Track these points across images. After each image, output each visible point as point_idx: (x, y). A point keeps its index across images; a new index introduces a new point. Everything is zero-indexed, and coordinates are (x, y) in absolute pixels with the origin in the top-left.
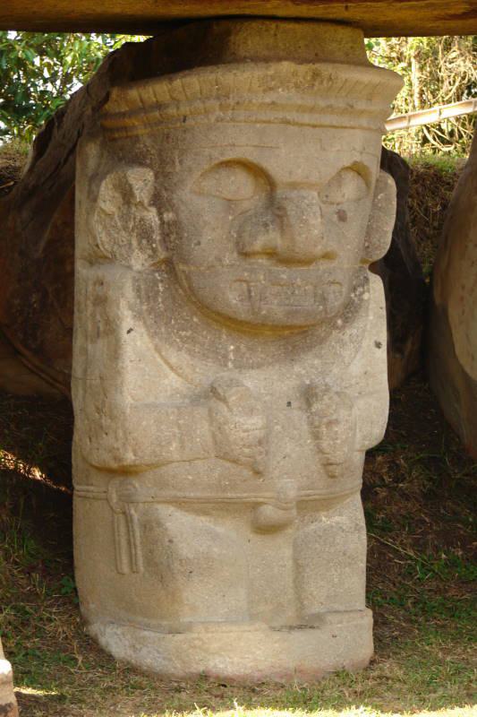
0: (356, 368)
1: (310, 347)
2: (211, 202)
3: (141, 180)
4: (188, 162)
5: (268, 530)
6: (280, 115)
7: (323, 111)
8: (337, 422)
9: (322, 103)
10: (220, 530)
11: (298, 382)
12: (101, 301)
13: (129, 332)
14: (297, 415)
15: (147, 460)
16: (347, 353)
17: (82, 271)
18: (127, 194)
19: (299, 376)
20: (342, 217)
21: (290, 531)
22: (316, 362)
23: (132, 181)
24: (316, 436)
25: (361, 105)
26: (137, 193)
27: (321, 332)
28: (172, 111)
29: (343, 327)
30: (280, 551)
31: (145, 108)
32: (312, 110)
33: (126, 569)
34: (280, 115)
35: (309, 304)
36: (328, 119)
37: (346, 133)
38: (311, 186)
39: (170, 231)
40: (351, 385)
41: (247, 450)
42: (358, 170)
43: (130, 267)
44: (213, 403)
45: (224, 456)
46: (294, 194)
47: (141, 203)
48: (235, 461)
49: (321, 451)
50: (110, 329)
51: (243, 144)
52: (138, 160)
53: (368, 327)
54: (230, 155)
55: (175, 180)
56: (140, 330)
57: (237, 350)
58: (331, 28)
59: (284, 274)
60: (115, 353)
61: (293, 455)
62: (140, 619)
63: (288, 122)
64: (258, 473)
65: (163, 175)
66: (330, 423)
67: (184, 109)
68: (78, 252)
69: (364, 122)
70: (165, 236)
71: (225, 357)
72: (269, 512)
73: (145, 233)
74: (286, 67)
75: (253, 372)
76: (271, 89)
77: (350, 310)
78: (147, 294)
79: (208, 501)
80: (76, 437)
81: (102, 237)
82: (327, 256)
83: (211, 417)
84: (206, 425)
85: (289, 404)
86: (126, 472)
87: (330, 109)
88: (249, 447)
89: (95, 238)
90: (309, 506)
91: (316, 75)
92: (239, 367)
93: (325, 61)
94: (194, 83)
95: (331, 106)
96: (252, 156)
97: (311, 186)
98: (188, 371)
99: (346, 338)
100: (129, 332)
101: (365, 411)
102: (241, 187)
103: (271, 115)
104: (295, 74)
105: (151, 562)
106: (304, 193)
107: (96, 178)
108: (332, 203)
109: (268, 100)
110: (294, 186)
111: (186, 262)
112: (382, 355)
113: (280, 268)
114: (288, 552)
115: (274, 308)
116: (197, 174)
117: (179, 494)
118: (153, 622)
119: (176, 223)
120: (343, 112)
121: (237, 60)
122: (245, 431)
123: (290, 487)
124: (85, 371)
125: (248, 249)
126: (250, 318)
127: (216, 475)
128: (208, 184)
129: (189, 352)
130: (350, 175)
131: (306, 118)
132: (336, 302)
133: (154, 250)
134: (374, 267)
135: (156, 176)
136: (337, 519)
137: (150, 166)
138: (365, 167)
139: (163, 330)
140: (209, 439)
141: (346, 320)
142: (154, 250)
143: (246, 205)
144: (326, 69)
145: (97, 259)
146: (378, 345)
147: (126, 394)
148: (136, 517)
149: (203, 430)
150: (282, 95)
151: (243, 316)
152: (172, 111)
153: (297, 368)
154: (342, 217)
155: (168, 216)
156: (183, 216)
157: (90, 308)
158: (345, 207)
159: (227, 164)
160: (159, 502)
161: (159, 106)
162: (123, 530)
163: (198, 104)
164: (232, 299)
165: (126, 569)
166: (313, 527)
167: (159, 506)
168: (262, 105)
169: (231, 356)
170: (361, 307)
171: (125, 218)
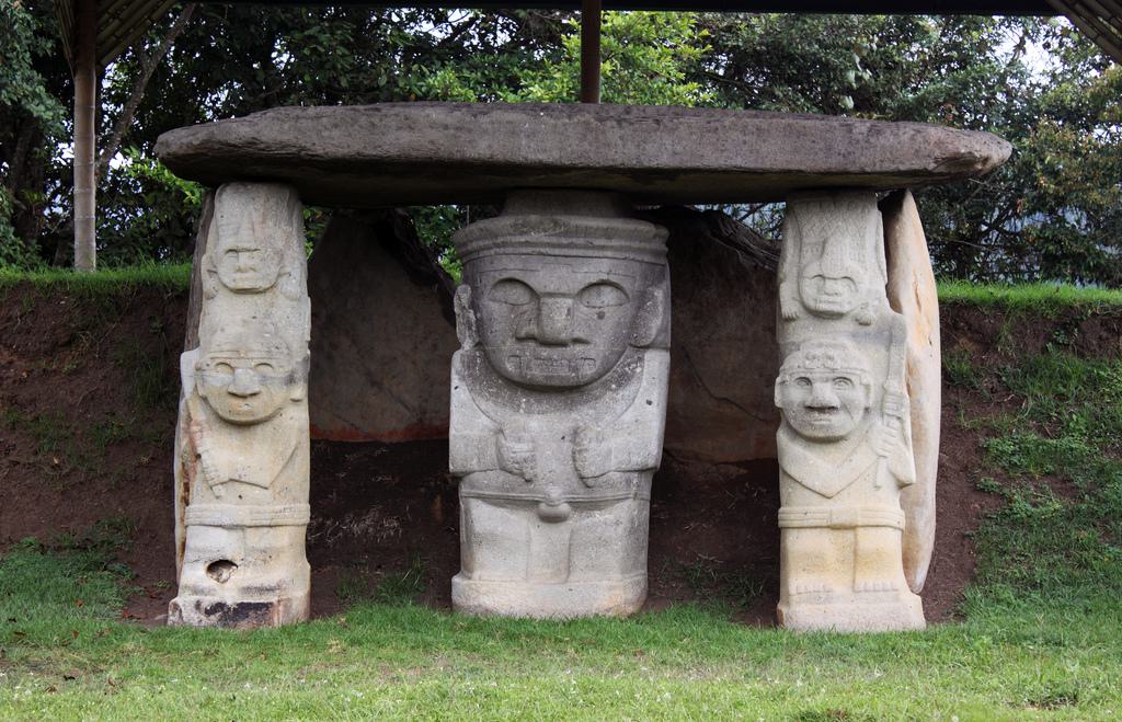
1: (587, 402)
2: (496, 307)
4: (483, 282)
5: (552, 519)
6: (538, 249)
8: (586, 450)
9: (564, 241)
10: (513, 517)
11: (573, 424)
13: (456, 388)
14: (567, 446)
16: (619, 408)
19: (575, 420)
20: (601, 316)
22: (591, 412)
24: (574, 460)
29: (616, 390)
30: (561, 533)
35: (564, 372)
37: (595, 260)
40: (622, 428)
41: (517, 466)
45: (504, 469)
46: (550, 301)
48: (511, 472)
49: (576, 470)
51: (511, 266)
53: (641, 390)
54: (505, 275)
55: (480, 291)
57: (528, 401)
59: (545, 352)
61: (558, 471)
64: (528, 481)
65: (474, 289)
66: (580, 451)
67: (474, 245)
69: (609, 254)
70: (477, 327)
71: (519, 406)
73: (470, 328)
74: (533, 218)
75: (539, 417)
76: (526, 233)
77: (614, 374)
78: (469, 364)
79: (498, 498)
82: (577, 341)
85: (563, 438)
87: (576, 246)
88: (518, 463)
90: (583, 506)
91: (556, 223)
92: (529, 412)
95: (572, 243)
96: (519, 276)
97: (564, 295)
98: (492, 414)
99: (619, 397)
100: (456, 388)
103: (530, 250)
106: (559, 300)
108: (594, 307)
109: (523, 240)
110: (551, 295)
113: (543, 349)
115: (537, 373)
116: (489, 288)
117: (481, 492)
120: (585, 247)
122: (514, 452)
125: (518, 336)
126: (520, 380)
127: (501, 479)
129: (495, 403)
131: (557, 251)
135: (472, 290)
136: (607, 516)
139: (478, 387)
140: (494, 456)
141: (620, 385)
143: (525, 308)
144: (563, 219)
146: (649, 403)
149: (492, 451)
150: (533, 237)
151: (516, 379)
153: (574, 415)
154: (601, 316)
158: (605, 310)
159: (512, 281)
160: (479, 497)
163: (481, 243)
164: (510, 367)
166: (588, 520)
167: (472, 500)
168: (519, 243)
169: (523, 406)
170: (633, 376)
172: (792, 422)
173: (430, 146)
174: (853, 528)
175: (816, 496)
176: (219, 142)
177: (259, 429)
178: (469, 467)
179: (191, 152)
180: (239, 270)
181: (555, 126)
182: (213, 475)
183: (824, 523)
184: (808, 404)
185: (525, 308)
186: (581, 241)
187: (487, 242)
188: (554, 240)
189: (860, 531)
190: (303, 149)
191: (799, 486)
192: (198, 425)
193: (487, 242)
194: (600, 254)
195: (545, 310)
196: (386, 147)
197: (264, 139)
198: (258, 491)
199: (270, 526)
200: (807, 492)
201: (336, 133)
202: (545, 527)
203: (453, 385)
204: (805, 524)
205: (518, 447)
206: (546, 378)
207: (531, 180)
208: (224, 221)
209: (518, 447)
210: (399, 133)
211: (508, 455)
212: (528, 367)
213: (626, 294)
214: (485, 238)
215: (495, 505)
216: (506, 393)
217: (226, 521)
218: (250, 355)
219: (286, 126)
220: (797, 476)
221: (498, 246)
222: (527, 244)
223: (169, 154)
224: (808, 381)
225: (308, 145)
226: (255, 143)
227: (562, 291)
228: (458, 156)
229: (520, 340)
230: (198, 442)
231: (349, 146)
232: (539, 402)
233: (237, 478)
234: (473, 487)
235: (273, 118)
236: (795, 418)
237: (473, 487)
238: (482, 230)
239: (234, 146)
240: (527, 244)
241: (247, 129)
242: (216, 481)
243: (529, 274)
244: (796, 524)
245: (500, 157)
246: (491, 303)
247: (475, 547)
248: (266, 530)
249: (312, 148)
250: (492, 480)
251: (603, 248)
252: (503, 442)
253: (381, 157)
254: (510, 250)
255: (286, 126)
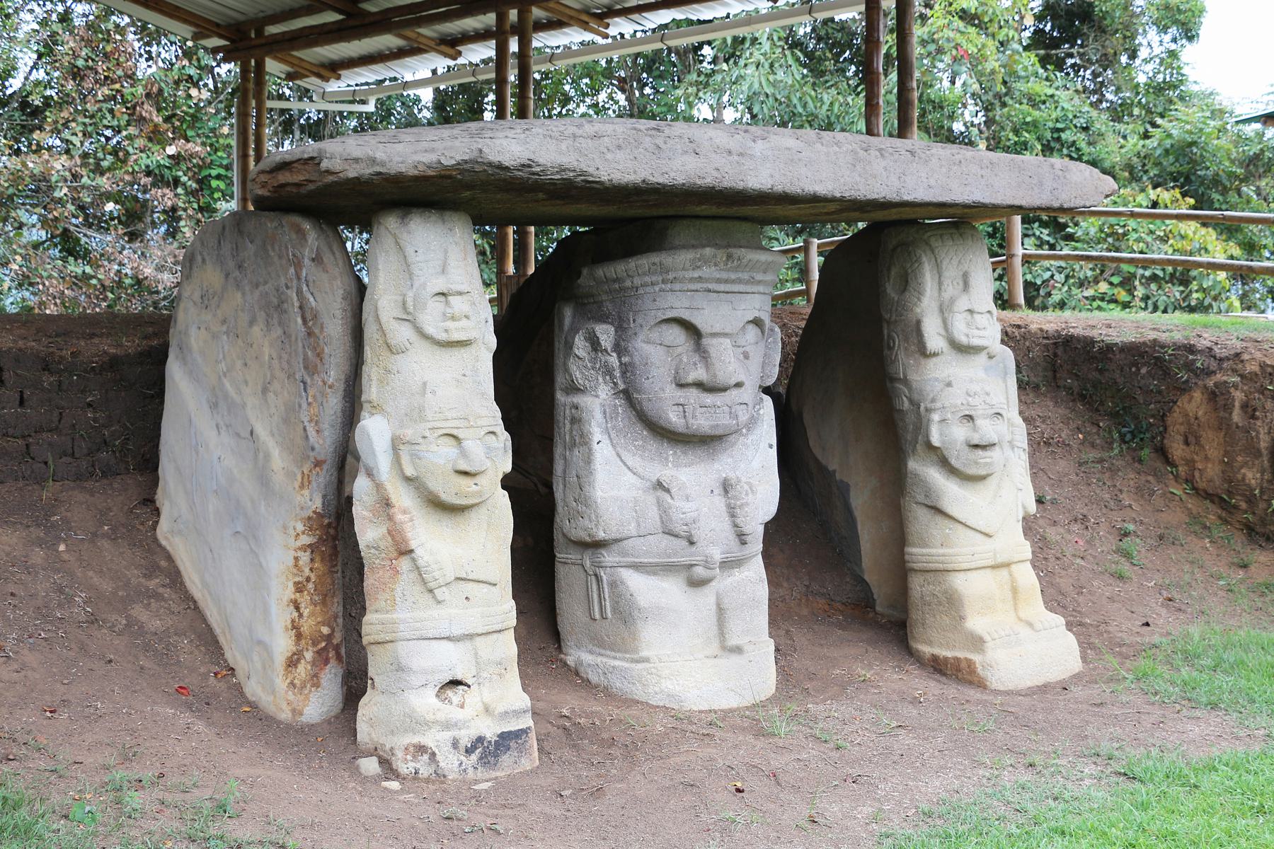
0: (756, 464)
2: (658, 353)
3: (606, 334)
4: (639, 321)
5: (697, 583)
6: (705, 286)
7: (733, 282)
8: (747, 504)
9: (733, 276)
12: (576, 421)
14: (719, 502)
15: (613, 536)
17: (560, 397)
18: (595, 344)
20: (746, 356)
21: (713, 583)
22: (730, 460)
23: (598, 334)
24: (733, 516)
25: (759, 277)
26: (603, 343)
27: (732, 438)
28: (628, 283)
30: (707, 597)
31: (608, 280)
32: (726, 281)
33: (597, 616)
34: (705, 286)
36: (736, 288)
38: (725, 335)
39: (626, 369)
42: (757, 322)
43: (597, 396)
44: (660, 493)
46: (714, 341)
47: (606, 350)
48: (676, 536)
49: (736, 526)
50: (583, 441)
51: (678, 305)
52: (603, 319)
54: (670, 315)
56: (606, 441)
58: (737, 223)
59: (709, 399)
60: (588, 461)
62: (608, 653)
63: (709, 291)
67: (637, 281)
68: (557, 386)
69: (761, 288)
70: (624, 373)
71: (667, 459)
72: (700, 571)
73: (609, 372)
74: (708, 251)
75: (687, 469)
77: (753, 422)
79: (657, 565)
80: (557, 519)
81: (577, 374)
82: (739, 385)
83: (659, 503)
84: (656, 509)
86: (598, 545)
87: (739, 281)
89: (571, 376)
90: (729, 564)
91: (729, 257)
92: (677, 466)
93: (735, 247)
94: (644, 261)
96: (685, 315)
97: (725, 335)
98: (640, 470)
101: (763, 494)
102: (676, 335)
104: (715, 256)
105: (614, 610)
106: (721, 340)
107: (574, 330)
109: (696, 275)
110: (714, 335)
111: (639, 392)
112: (773, 453)
113: (705, 395)
114: (712, 600)
116: (646, 329)
118: (618, 655)
119: (631, 364)
120: (747, 282)
121: (673, 248)
123: (717, 555)
124: (565, 471)
125: (683, 382)
128: (654, 335)
130: (751, 326)
131: (722, 287)
132: (743, 418)
133: (615, 384)
134: (767, 390)
136: (746, 573)
137: (612, 324)
138: (761, 320)
142: (615, 384)
145: (574, 389)
147: (597, 488)
148: (605, 578)
149: (653, 514)
150: (706, 271)
152: (628, 283)
153: (717, 466)
154: (746, 356)
155: (625, 359)
156: (637, 359)
157: (568, 426)
158: (747, 349)
161: (617, 280)
162: (595, 587)
163: (647, 279)
164: (674, 418)
165: (597, 616)
166: (730, 580)
171: (593, 361)
172: (953, 462)
173: (715, 174)
174: (1007, 565)
175: (979, 536)
176: (490, 164)
177: (473, 514)
178: (626, 533)
179: (430, 173)
180: (453, 318)
181: (827, 154)
182: (437, 574)
183: (991, 563)
184: (976, 442)
185: (680, 350)
186: (745, 276)
187: (654, 278)
188: (724, 275)
189: (1013, 566)
190: (583, 173)
191: (960, 527)
192: (405, 512)
193: (654, 278)
194: (755, 289)
195: (713, 352)
196: (672, 175)
197: (541, 161)
198: (485, 588)
199: (500, 631)
200: (972, 533)
201: (620, 155)
202: (690, 590)
203: (596, 439)
204: (973, 565)
205: (687, 506)
206: (712, 427)
207: (734, 211)
208: (420, 257)
209: (687, 506)
210: (685, 157)
211: (676, 516)
212: (694, 417)
213: (763, 332)
214: (655, 273)
215: (648, 573)
216: (653, 445)
217: (457, 631)
218: (480, 423)
219: (564, 146)
220: (951, 513)
221: (664, 282)
222: (700, 279)
223: (380, 173)
224: (970, 418)
225: (591, 170)
226: (530, 166)
227: (727, 331)
228: (741, 185)
229: (681, 386)
230: (409, 535)
231: (635, 172)
232: (685, 453)
233: (464, 576)
234: (624, 554)
235: (545, 136)
236: (958, 458)
237: (625, 554)
238: (654, 264)
239: (507, 168)
240: (700, 279)
241: (519, 149)
242: (441, 582)
243: (696, 312)
244: (965, 566)
245: (779, 188)
246: (644, 345)
247: (640, 624)
248: (495, 636)
249: (595, 173)
250: (657, 547)
251: (759, 282)
252: (670, 500)
253: (664, 186)
254: (677, 286)
255: (564, 146)
